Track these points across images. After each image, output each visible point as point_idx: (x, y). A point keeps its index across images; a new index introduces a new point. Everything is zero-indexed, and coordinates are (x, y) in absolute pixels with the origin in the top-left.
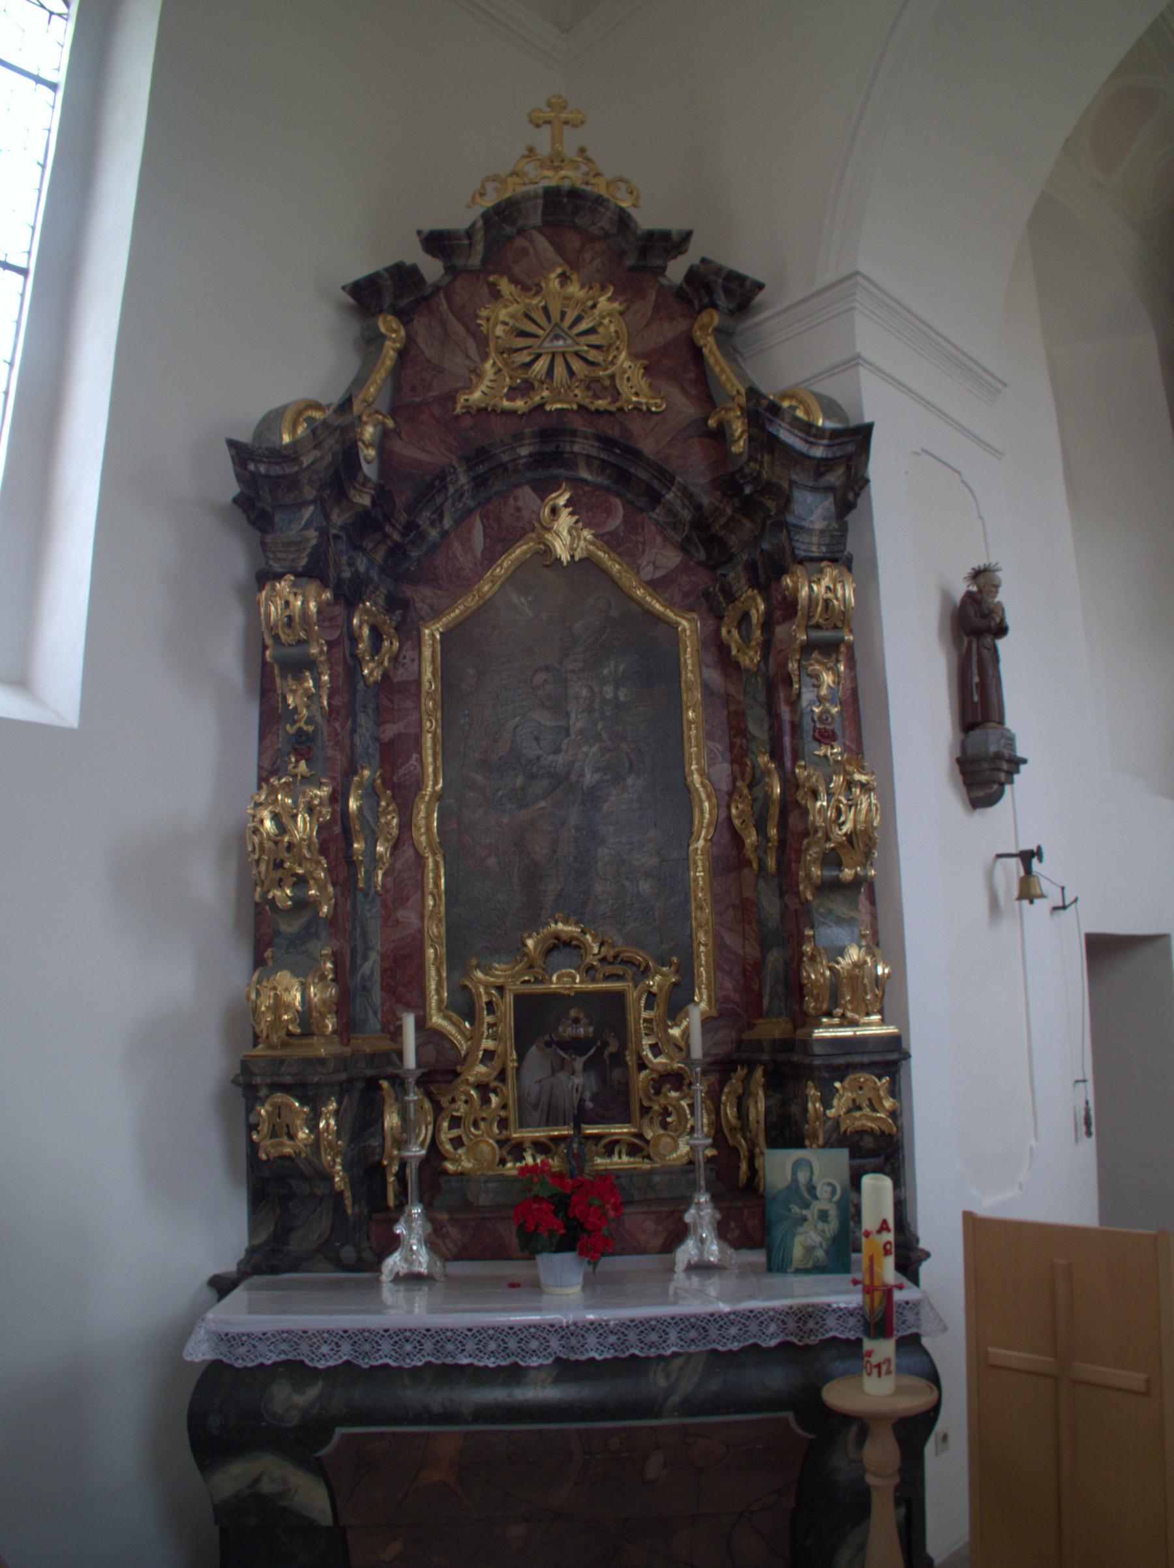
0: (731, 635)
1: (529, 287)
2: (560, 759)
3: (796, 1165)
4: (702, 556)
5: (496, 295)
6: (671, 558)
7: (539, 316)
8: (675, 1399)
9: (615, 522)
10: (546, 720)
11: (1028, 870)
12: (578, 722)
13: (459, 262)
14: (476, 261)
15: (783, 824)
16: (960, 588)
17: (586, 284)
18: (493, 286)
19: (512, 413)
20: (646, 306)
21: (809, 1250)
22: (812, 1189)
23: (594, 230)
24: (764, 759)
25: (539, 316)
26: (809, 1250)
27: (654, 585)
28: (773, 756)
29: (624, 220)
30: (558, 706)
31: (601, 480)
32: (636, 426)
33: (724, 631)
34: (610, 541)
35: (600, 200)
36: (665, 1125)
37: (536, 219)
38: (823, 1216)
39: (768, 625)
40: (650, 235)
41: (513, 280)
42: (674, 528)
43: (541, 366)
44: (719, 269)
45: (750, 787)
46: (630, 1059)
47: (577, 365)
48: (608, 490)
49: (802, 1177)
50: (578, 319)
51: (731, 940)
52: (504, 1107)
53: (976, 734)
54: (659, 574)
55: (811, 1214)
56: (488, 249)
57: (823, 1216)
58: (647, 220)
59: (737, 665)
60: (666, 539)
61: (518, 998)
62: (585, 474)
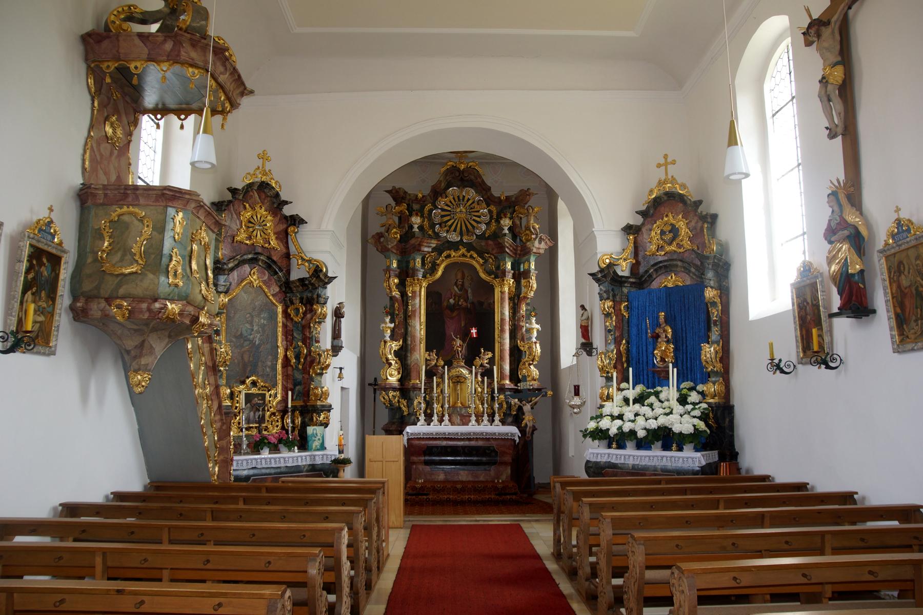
0: (292, 314)
1: (253, 208)
2: (252, 337)
3: (313, 430)
4: (284, 289)
5: (245, 208)
6: (277, 289)
7: (255, 217)
8: (305, 469)
9: (266, 278)
10: (247, 325)
11: (341, 372)
12: (255, 328)
13: (237, 197)
14: (241, 197)
15: (305, 359)
16: (336, 305)
17: (266, 210)
18: (245, 206)
19: (247, 244)
20: (277, 219)
21: (316, 446)
22: (317, 434)
23: (269, 194)
24: (300, 344)
25: (255, 217)
26: (316, 446)
27: (273, 295)
28: (303, 344)
29: (277, 195)
30: (251, 323)
31: (264, 266)
32: (273, 253)
33: (289, 310)
34: (265, 282)
35: (273, 188)
36: (272, 424)
37: (256, 188)
38: (319, 439)
39: (305, 314)
40: (284, 201)
41: (250, 206)
42: (279, 281)
43: (255, 233)
44: (300, 217)
45: (294, 349)
46: (266, 409)
47: (262, 234)
48: (265, 269)
49: (315, 432)
50: (264, 221)
51: (284, 383)
52: (240, 420)
53: (336, 341)
54: (275, 292)
55: (316, 439)
56: (244, 195)
57: (319, 439)
58: (283, 197)
59: (292, 319)
60: (277, 284)
61: (245, 394)
62: (260, 264)
